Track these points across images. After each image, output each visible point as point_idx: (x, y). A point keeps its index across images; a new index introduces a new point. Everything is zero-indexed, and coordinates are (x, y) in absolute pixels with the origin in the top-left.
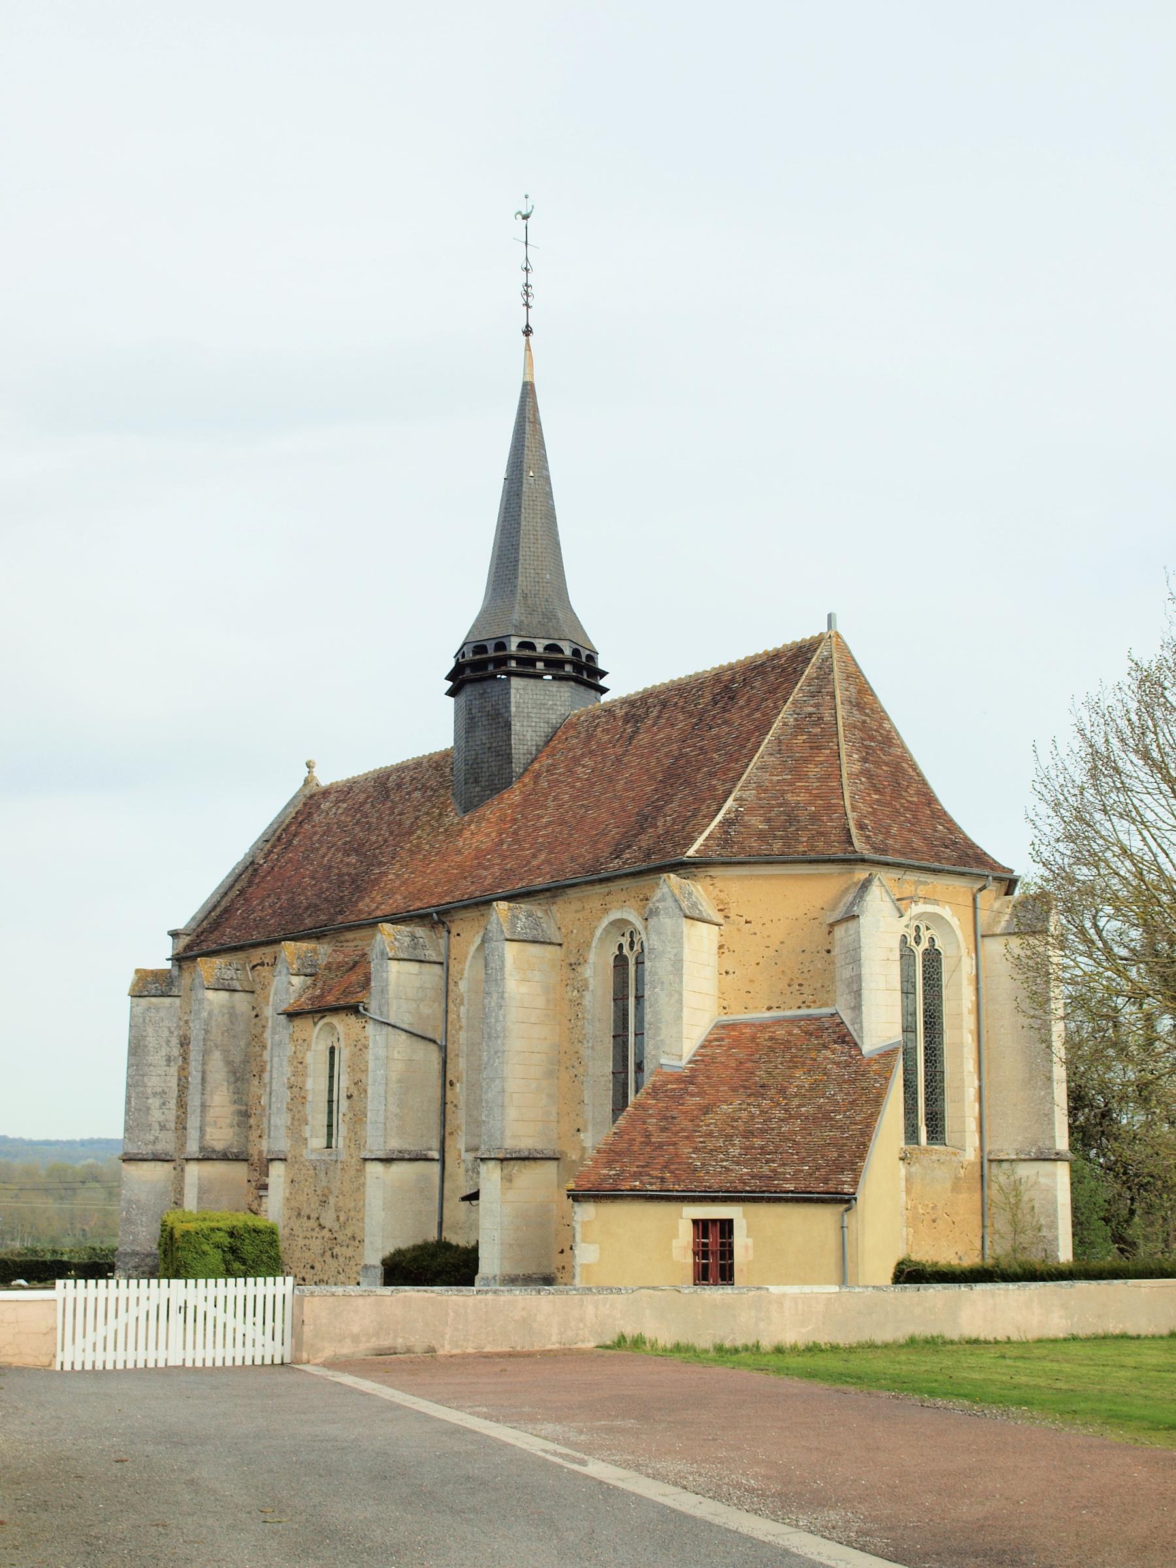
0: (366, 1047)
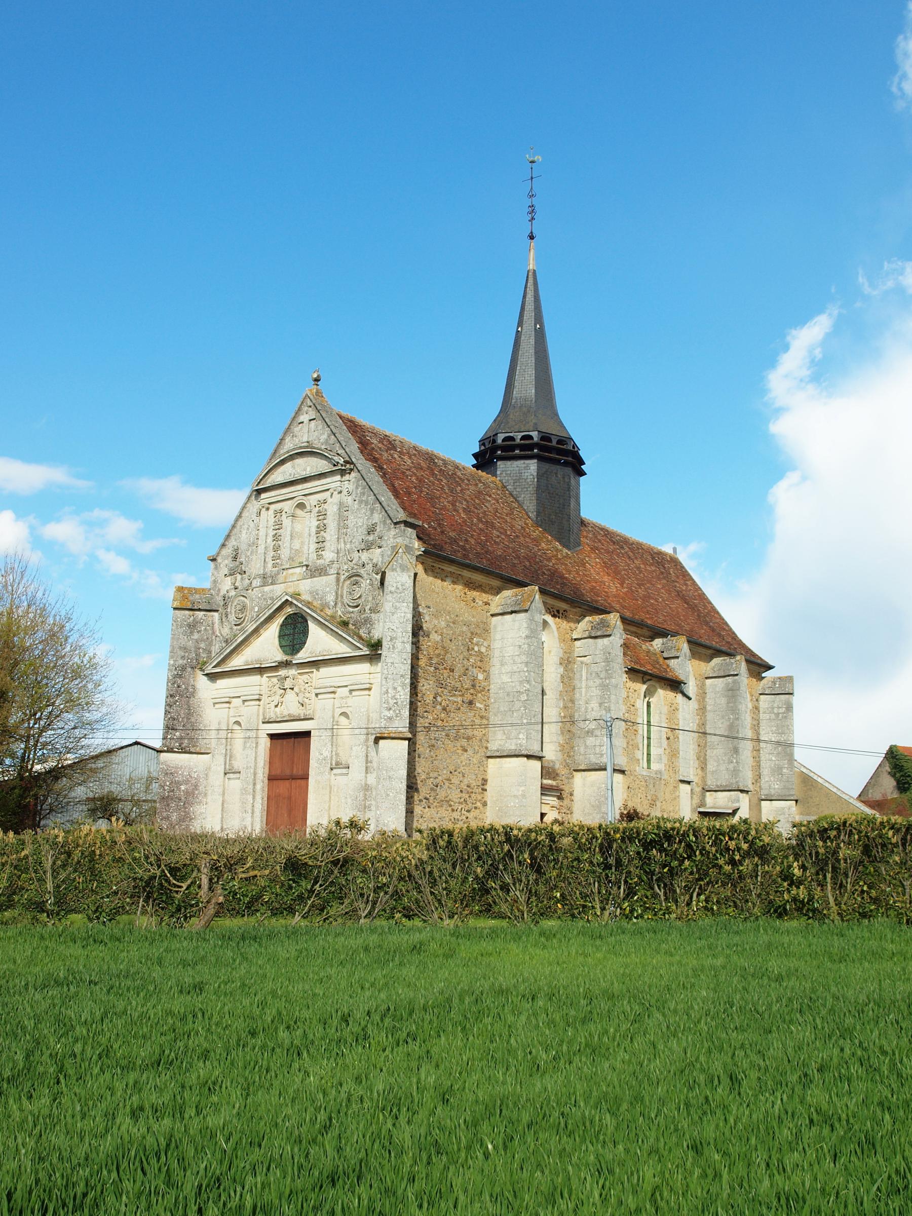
0: (677, 710)
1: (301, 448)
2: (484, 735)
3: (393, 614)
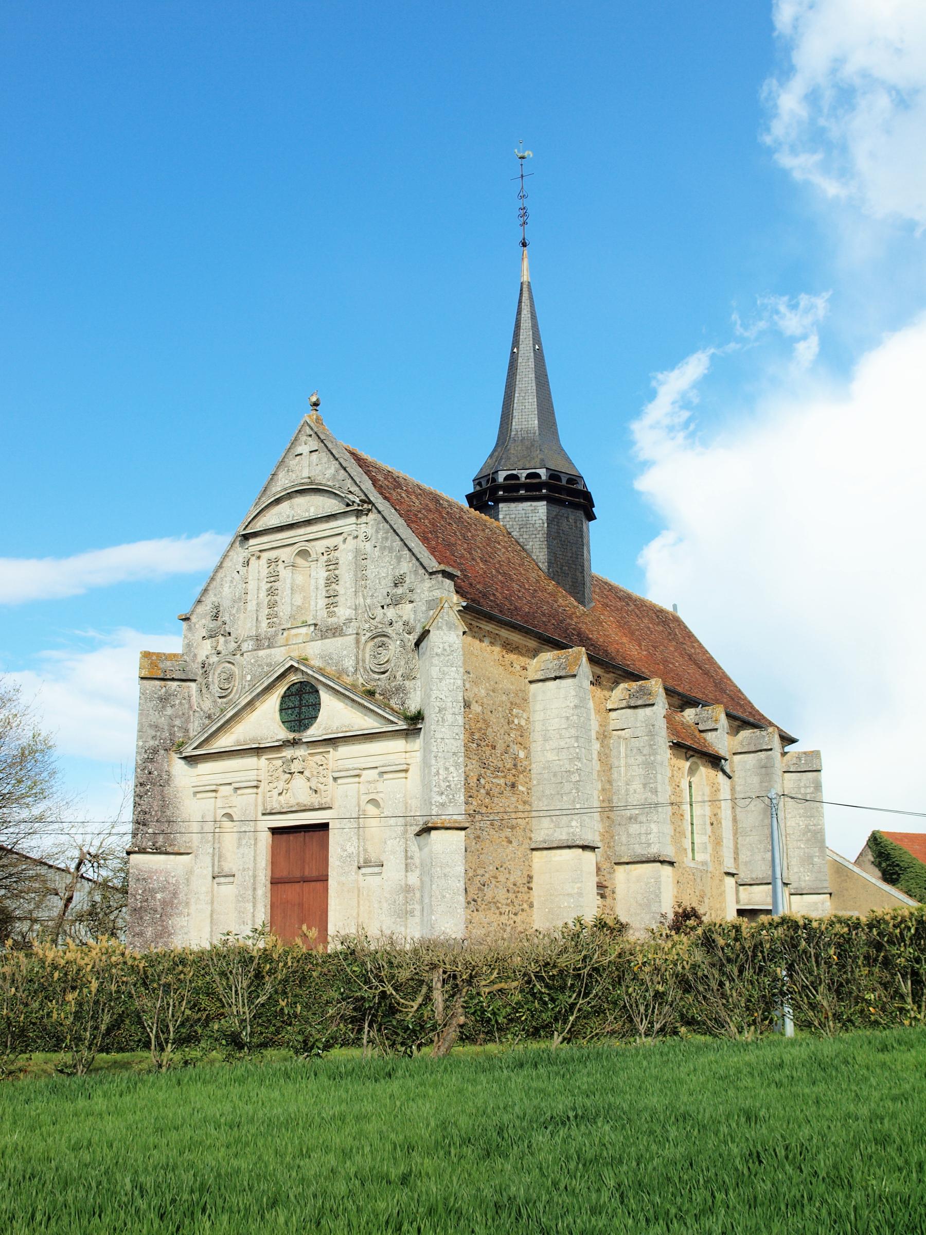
0: (719, 790)
1: (302, 484)
2: (528, 823)
3: (441, 680)
